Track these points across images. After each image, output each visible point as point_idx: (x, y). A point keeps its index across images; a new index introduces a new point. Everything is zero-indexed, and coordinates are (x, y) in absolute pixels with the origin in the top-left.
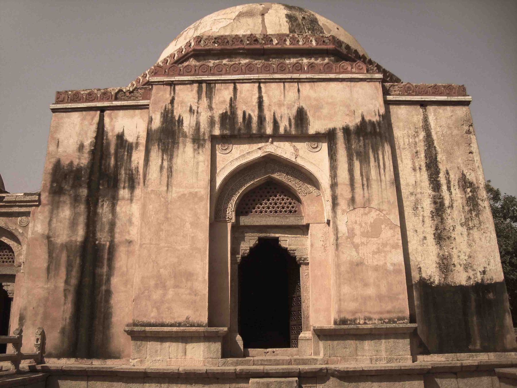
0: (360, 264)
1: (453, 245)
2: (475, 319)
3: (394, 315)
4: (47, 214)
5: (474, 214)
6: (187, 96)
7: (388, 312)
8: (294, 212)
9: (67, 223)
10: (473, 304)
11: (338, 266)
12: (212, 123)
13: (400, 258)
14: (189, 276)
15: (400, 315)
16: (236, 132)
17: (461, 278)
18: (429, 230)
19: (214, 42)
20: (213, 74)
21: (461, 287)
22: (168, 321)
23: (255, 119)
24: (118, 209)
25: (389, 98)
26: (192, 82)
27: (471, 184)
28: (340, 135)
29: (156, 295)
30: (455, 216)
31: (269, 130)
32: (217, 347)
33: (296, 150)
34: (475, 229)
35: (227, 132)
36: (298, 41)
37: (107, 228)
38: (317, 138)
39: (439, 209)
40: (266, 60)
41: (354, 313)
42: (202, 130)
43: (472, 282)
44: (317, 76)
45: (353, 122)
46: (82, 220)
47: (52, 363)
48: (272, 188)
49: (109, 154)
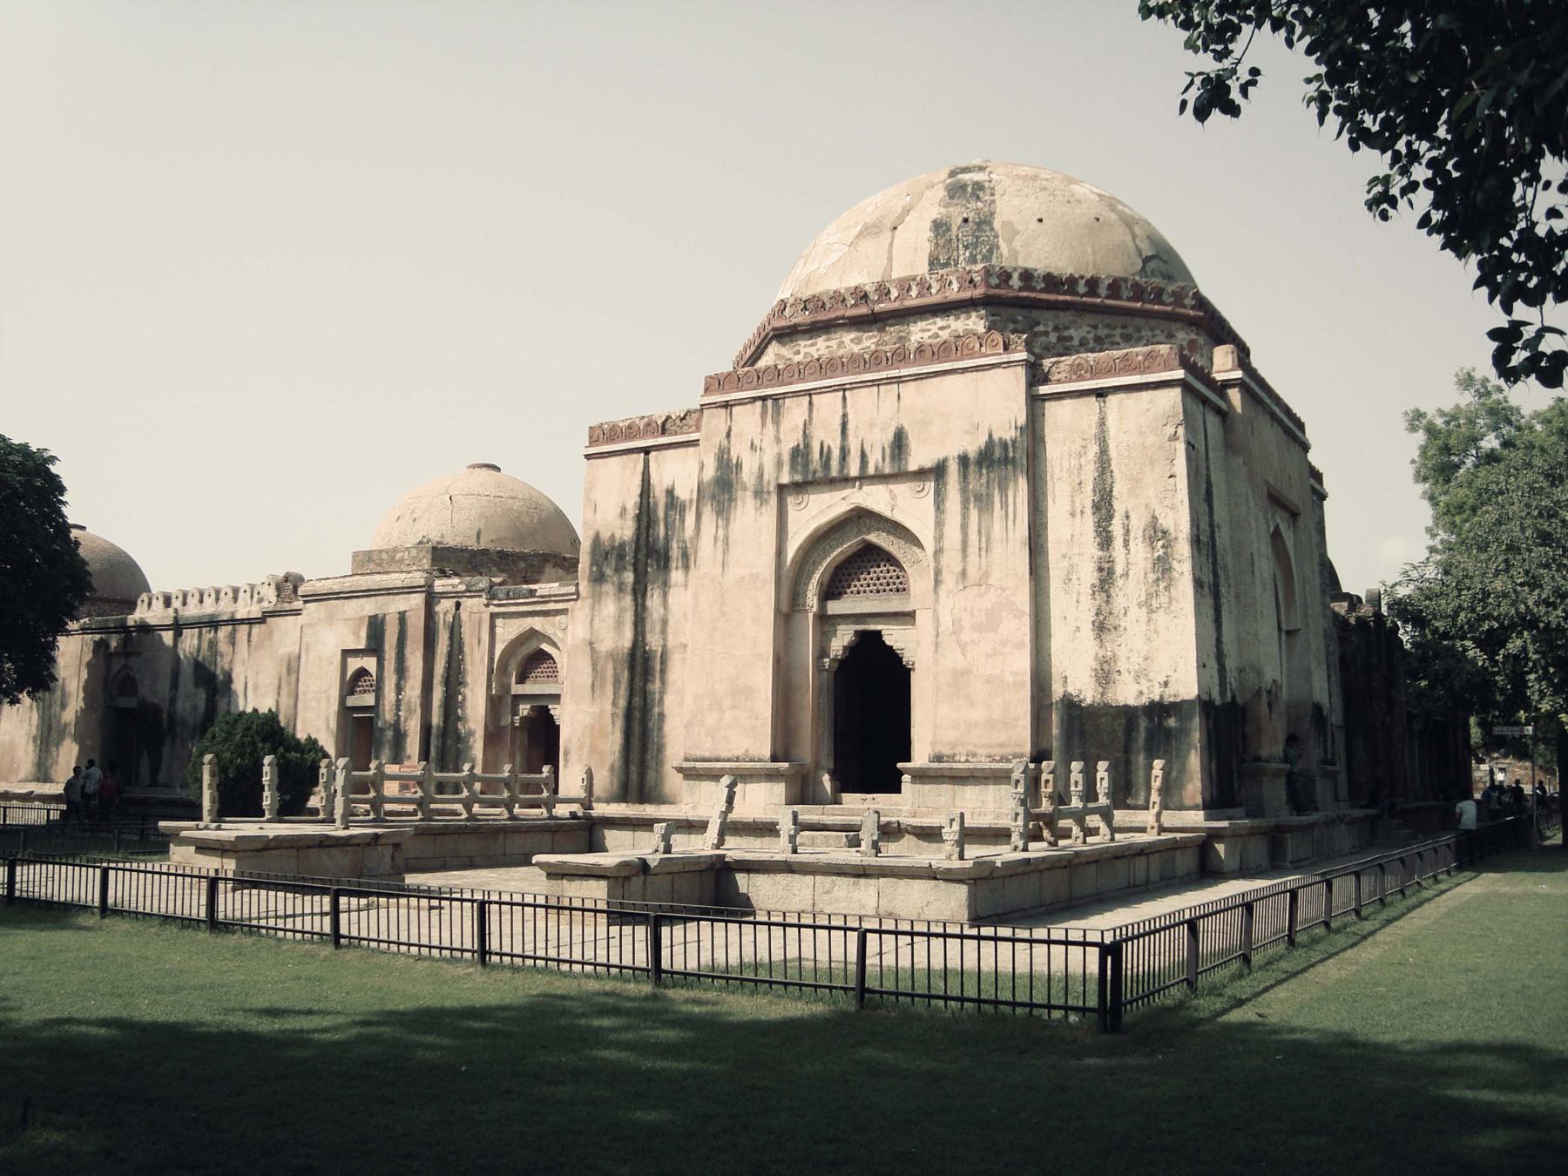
0: (966, 673)
1: (1120, 640)
2: (1141, 758)
3: (1010, 750)
4: (587, 610)
5: (1162, 585)
6: (747, 420)
7: (1001, 745)
8: (902, 590)
9: (611, 621)
10: (1142, 735)
11: (936, 677)
12: (779, 464)
13: (1022, 663)
14: (748, 692)
15: (1017, 750)
16: (810, 478)
17: (1127, 693)
18: (1086, 617)
19: (805, 308)
20: (783, 384)
21: (1126, 707)
22: (725, 755)
23: (836, 454)
24: (670, 600)
25: (1044, 390)
26: (755, 399)
27: (1164, 532)
28: (953, 469)
29: (711, 719)
30: (1129, 592)
31: (854, 470)
32: (779, 789)
33: (894, 497)
34: (1161, 612)
35: (799, 478)
36: (929, 288)
37: (658, 627)
38: (921, 474)
39: (1106, 578)
40: (881, 330)
41: (954, 746)
42: (766, 477)
43: (1144, 700)
44: (925, 369)
45: (973, 446)
46: (629, 617)
47: (601, 810)
48: (870, 555)
49: (656, 521)
